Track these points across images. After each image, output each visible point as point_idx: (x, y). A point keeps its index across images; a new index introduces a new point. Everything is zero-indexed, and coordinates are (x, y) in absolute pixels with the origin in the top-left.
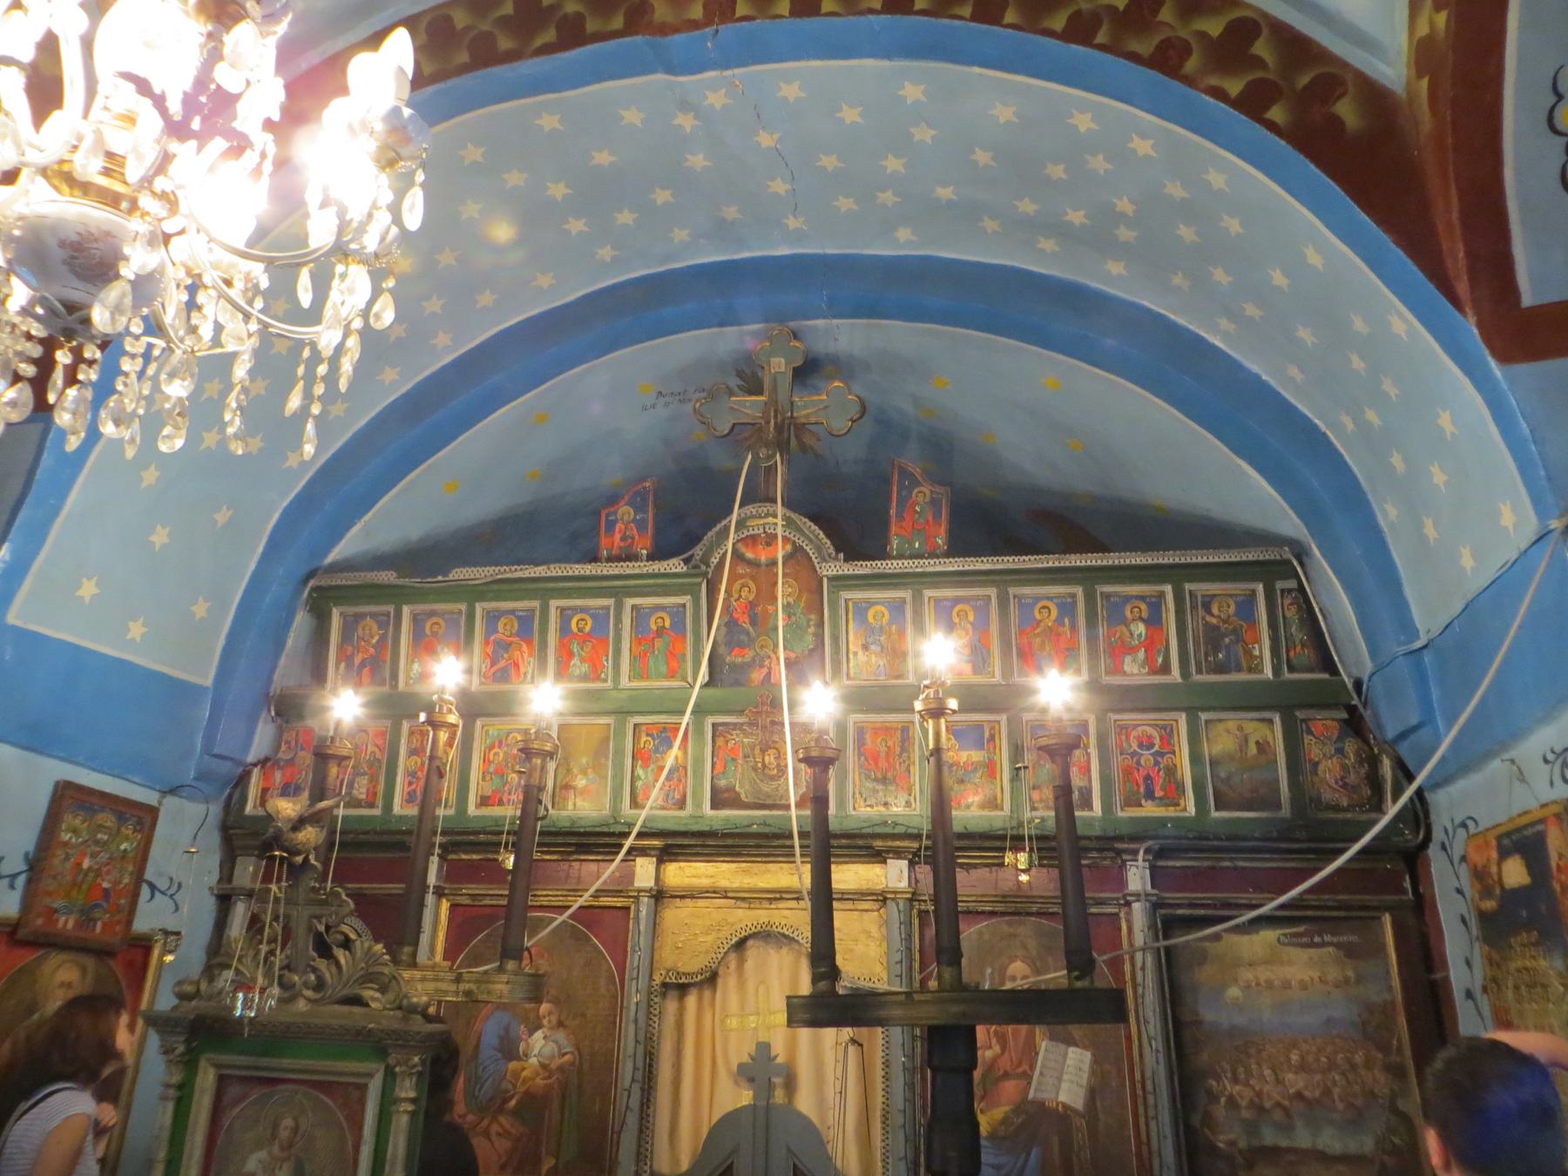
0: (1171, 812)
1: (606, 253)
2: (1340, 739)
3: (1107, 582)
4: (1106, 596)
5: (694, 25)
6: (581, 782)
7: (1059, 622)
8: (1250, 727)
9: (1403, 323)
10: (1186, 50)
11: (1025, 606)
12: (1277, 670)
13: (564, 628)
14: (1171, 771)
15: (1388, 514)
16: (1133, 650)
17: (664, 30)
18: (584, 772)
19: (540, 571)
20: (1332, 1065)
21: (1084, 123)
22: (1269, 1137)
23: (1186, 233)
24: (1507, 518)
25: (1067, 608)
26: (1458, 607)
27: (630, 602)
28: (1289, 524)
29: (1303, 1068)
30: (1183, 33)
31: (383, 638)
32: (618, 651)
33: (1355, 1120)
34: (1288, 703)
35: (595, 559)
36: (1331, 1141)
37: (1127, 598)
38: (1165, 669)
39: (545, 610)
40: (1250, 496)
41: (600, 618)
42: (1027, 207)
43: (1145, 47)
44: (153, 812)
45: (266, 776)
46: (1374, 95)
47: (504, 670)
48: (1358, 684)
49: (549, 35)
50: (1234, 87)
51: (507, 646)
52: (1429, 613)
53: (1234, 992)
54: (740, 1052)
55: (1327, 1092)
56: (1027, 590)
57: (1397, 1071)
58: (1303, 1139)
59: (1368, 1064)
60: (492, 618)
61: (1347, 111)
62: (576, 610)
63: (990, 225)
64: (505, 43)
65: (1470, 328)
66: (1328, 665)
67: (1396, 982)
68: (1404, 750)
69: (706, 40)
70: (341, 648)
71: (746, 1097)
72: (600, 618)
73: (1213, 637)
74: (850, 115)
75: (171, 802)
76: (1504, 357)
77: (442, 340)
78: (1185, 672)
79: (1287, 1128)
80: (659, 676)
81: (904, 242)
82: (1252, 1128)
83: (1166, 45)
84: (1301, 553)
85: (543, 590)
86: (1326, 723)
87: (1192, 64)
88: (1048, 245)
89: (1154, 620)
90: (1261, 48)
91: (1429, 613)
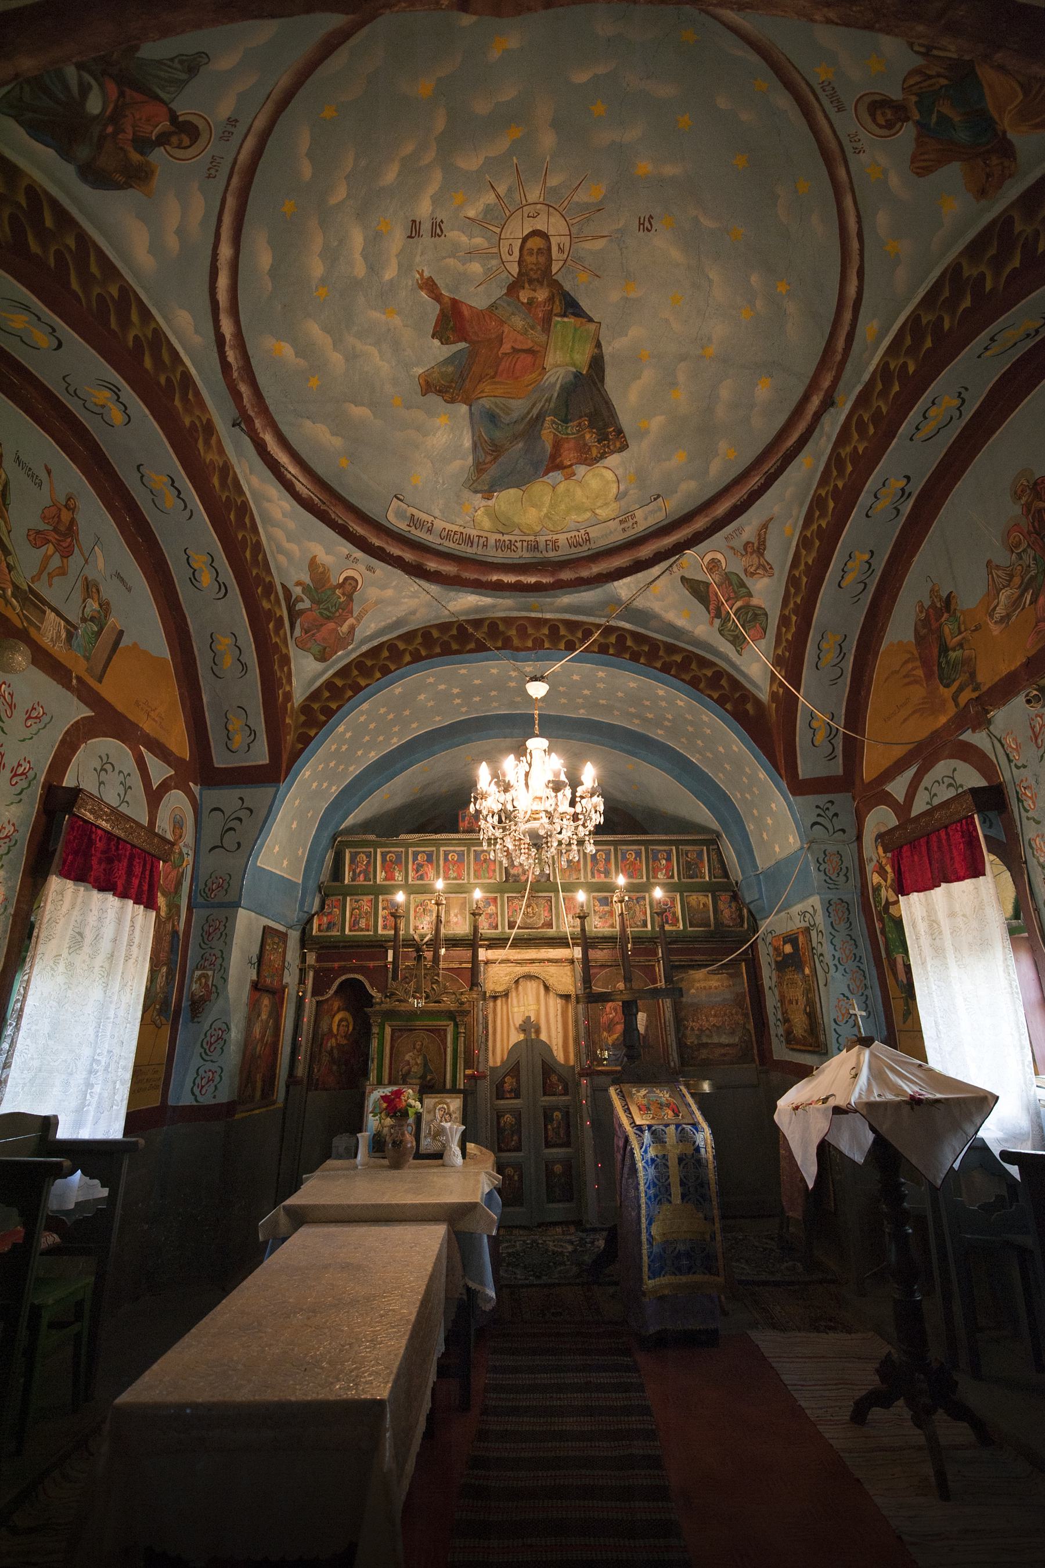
0: (674, 928)
1: (464, 709)
2: (731, 902)
3: (653, 845)
4: (652, 850)
5: (528, 649)
6: (455, 920)
7: (635, 859)
8: (701, 898)
9: (762, 775)
10: (700, 681)
11: (624, 854)
12: (710, 878)
13: (446, 859)
14: (674, 913)
15: (750, 827)
16: (661, 870)
17: (517, 649)
18: (456, 916)
19: (438, 836)
20: (725, 1014)
21: (661, 693)
22: (705, 1040)
23: (690, 729)
24: (791, 840)
25: (638, 854)
26: (773, 862)
27: (473, 849)
28: (715, 825)
29: (715, 1016)
30: (699, 674)
31: (369, 862)
32: (469, 868)
33: (733, 1033)
34: (712, 889)
35: (457, 832)
36: (725, 1040)
37: (660, 851)
38: (672, 877)
39: (438, 851)
40: (703, 814)
41: (461, 855)
42: (633, 710)
43: (687, 677)
44: (286, 935)
45: (320, 920)
46: (757, 702)
47: (421, 875)
48: (737, 883)
49: (472, 646)
50: (716, 696)
51: (421, 866)
52: (763, 863)
53: (693, 991)
54: (518, 1021)
55: (724, 1023)
56: (624, 847)
57: (746, 1015)
58: (716, 1040)
59: (736, 1014)
60: (416, 855)
61: (749, 707)
62: (450, 851)
63: (616, 713)
64: (455, 646)
65: (784, 785)
66: (726, 875)
67: (746, 985)
68: (751, 907)
69: (533, 654)
70: (350, 866)
71: (522, 1037)
72: (461, 855)
73: (688, 865)
74: (576, 677)
75: (290, 931)
76: (794, 794)
77: (395, 740)
78: (679, 879)
79: (710, 1036)
80: (485, 878)
81: (582, 714)
82: (699, 1037)
83: (694, 677)
84: (719, 836)
85: (437, 844)
86: (725, 897)
87: (702, 685)
88: (637, 721)
89: (669, 859)
90: (724, 682)
91: (763, 863)
